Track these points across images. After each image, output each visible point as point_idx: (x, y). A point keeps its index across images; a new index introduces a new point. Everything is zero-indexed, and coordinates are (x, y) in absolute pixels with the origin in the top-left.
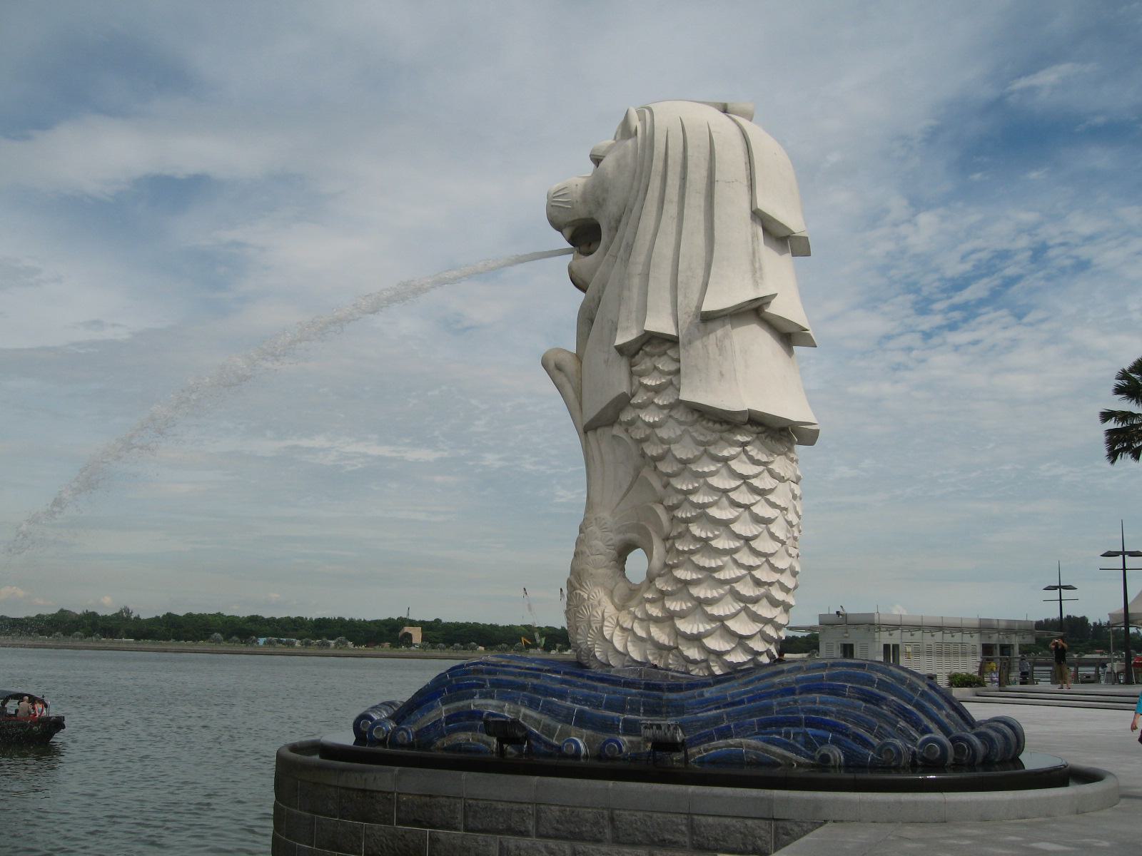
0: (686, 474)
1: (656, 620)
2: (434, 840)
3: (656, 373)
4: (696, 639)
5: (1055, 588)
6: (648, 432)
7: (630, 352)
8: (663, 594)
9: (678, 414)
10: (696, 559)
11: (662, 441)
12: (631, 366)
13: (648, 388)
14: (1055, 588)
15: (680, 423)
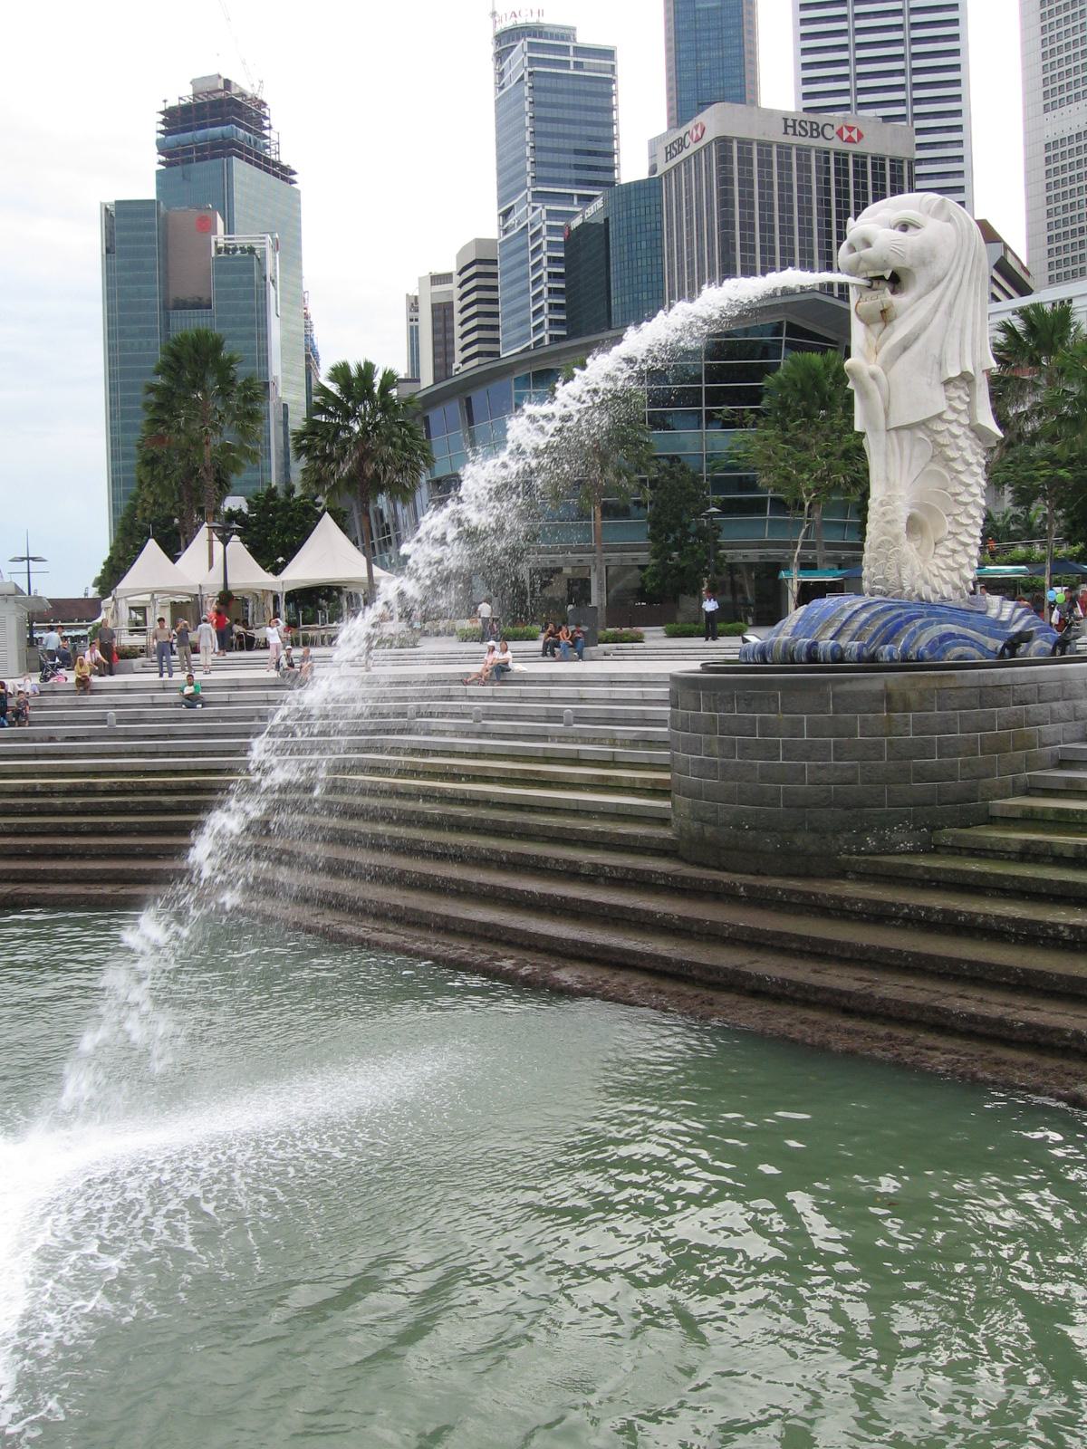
0: (967, 473)
1: (953, 570)
2: (1028, 712)
3: (957, 401)
4: (966, 581)
5: (23, 559)
6: (952, 440)
7: (947, 383)
8: (954, 551)
9: (969, 433)
10: (969, 529)
11: (959, 449)
12: (946, 391)
13: (955, 410)
14: (23, 559)
15: (967, 438)
